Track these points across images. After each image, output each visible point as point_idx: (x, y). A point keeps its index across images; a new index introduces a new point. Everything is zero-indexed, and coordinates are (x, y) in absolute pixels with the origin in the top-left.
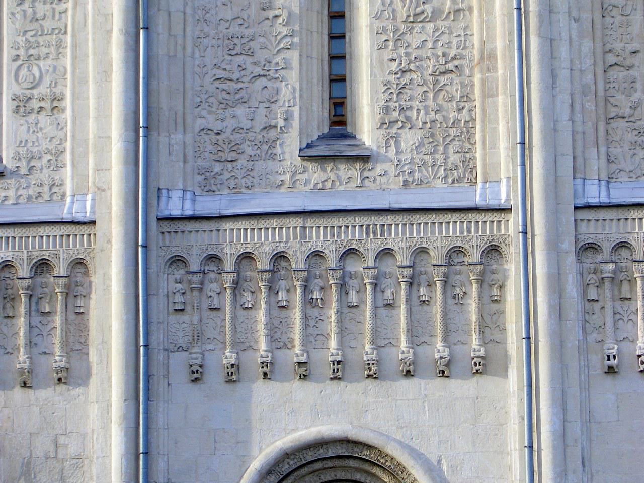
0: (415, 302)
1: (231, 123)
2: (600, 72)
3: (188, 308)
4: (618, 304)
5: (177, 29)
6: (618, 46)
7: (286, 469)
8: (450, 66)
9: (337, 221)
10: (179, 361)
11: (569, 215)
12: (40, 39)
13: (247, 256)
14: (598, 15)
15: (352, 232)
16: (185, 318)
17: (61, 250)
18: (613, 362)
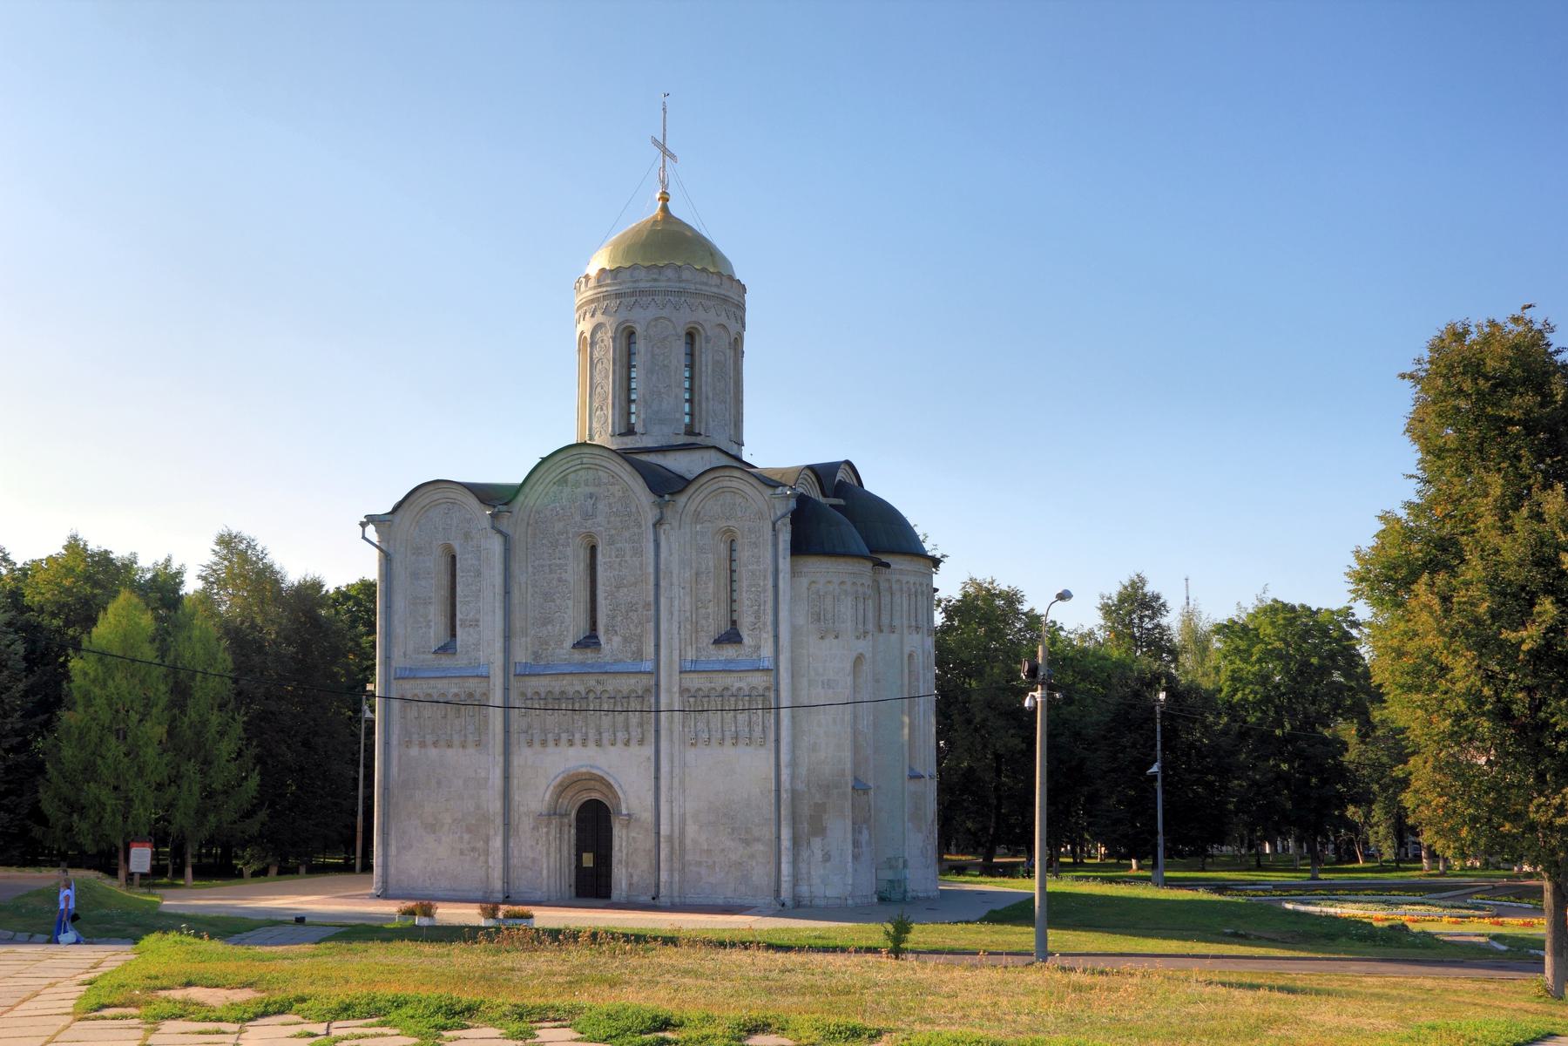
11: (676, 677)
15: (591, 681)
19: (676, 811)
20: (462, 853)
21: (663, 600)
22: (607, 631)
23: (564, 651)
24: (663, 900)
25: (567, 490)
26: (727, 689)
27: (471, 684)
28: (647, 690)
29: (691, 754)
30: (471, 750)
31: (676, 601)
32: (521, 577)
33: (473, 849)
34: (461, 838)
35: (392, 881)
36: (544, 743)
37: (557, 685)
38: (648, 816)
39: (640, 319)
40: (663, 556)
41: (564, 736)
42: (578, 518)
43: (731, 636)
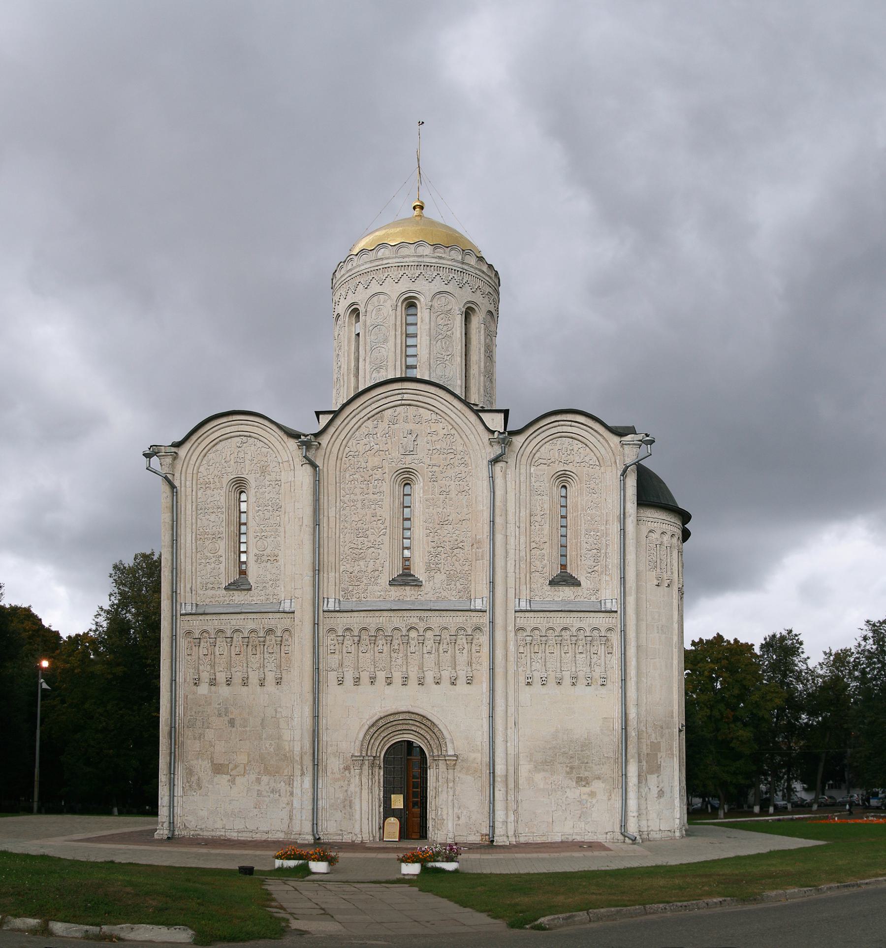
0: (441, 651)
1: (357, 568)
2: (528, 551)
3: (337, 652)
4: (533, 654)
5: (332, 525)
6: (537, 539)
7: (380, 723)
8: (460, 545)
9: (405, 614)
10: (332, 677)
11: (511, 615)
12: (268, 529)
13: (364, 629)
14: (528, 525)
16: (336, 656)
17: (278, 623)
18: (529, 680)
19: (511, 751)
20: (259, 793)
21: (499, 538)
22: (428, 569)
23: (380, 591)
24: (499, 840)
25: (383, 426)
26: (565, 629)
27: (272, 621)
28: (478, 629)
29: (526, 694)
30: (271, 687)
31: (512, 540)
32: (330, 512)
33: (273, 791)
34: (258, 781)
35: (178, 821)
36: (357, 681)
37: (373, 621)
38: (480, 757)
39: (425, 290)
40: (499, 493)
41: (381, 676)
42: (395, 454)
43: (564, 579)
